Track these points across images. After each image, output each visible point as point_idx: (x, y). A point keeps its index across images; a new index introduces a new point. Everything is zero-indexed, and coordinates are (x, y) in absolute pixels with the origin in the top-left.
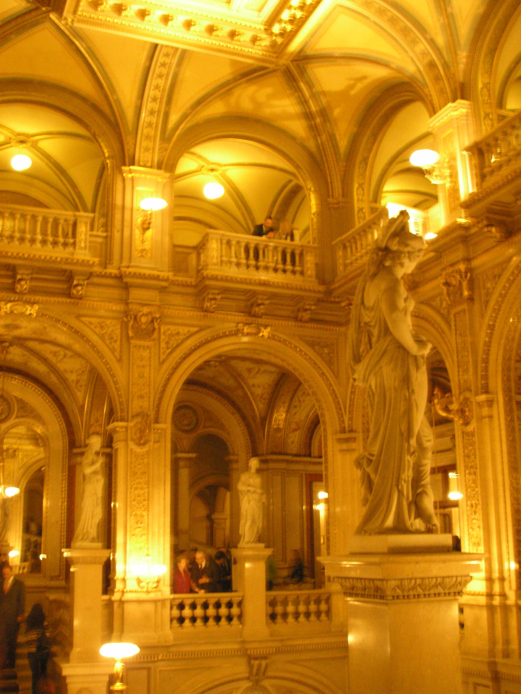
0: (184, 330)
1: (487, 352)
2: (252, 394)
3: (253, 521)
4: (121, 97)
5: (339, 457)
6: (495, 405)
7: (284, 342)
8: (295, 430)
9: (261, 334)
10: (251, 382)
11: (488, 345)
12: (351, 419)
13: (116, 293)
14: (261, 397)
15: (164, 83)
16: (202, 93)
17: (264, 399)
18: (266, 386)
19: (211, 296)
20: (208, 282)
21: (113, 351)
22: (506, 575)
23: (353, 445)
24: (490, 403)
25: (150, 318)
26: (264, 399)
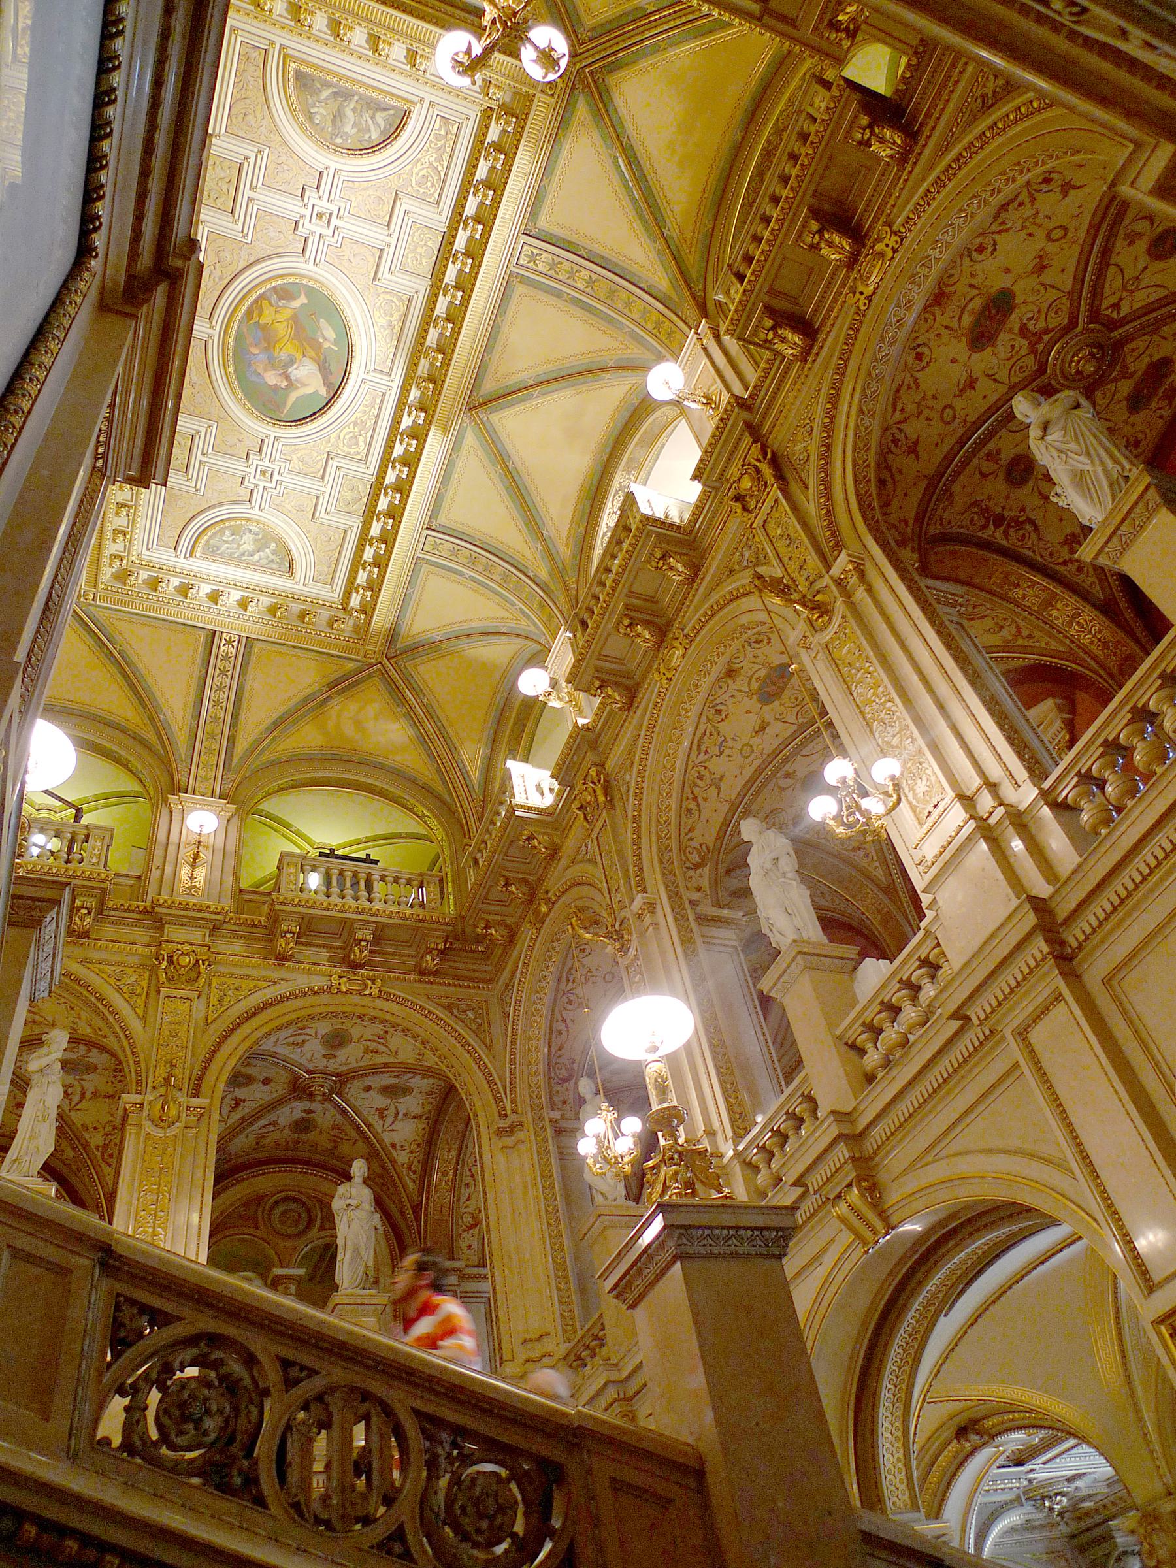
0: (247, 985)
1: (638, 853)
2: (394, 1162)
3: (357, 1253)
4: (169, 716)
5: (501, 1159)
6: (659, 907)
7: (404, 1003)
8: (472, 1227)
9: (367, 992)
10: (388, 1138)
11: (637, 844)
12: (514, 1101)
13: (144, 935)
14: (409, 1168)
15: (227, 698)
16: (281, 711)
17: (415, 1172)
18: (414, 1147)
19: (284, 928)
20: (278, 907)
21: (134, 1008)
22: (716, 1125)
23: (520, 1135)
24: (651, 907)
25: (192, 958)
26: (415, 1172)
